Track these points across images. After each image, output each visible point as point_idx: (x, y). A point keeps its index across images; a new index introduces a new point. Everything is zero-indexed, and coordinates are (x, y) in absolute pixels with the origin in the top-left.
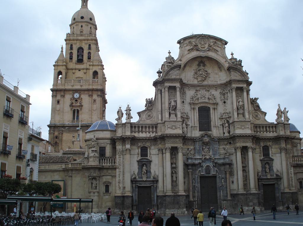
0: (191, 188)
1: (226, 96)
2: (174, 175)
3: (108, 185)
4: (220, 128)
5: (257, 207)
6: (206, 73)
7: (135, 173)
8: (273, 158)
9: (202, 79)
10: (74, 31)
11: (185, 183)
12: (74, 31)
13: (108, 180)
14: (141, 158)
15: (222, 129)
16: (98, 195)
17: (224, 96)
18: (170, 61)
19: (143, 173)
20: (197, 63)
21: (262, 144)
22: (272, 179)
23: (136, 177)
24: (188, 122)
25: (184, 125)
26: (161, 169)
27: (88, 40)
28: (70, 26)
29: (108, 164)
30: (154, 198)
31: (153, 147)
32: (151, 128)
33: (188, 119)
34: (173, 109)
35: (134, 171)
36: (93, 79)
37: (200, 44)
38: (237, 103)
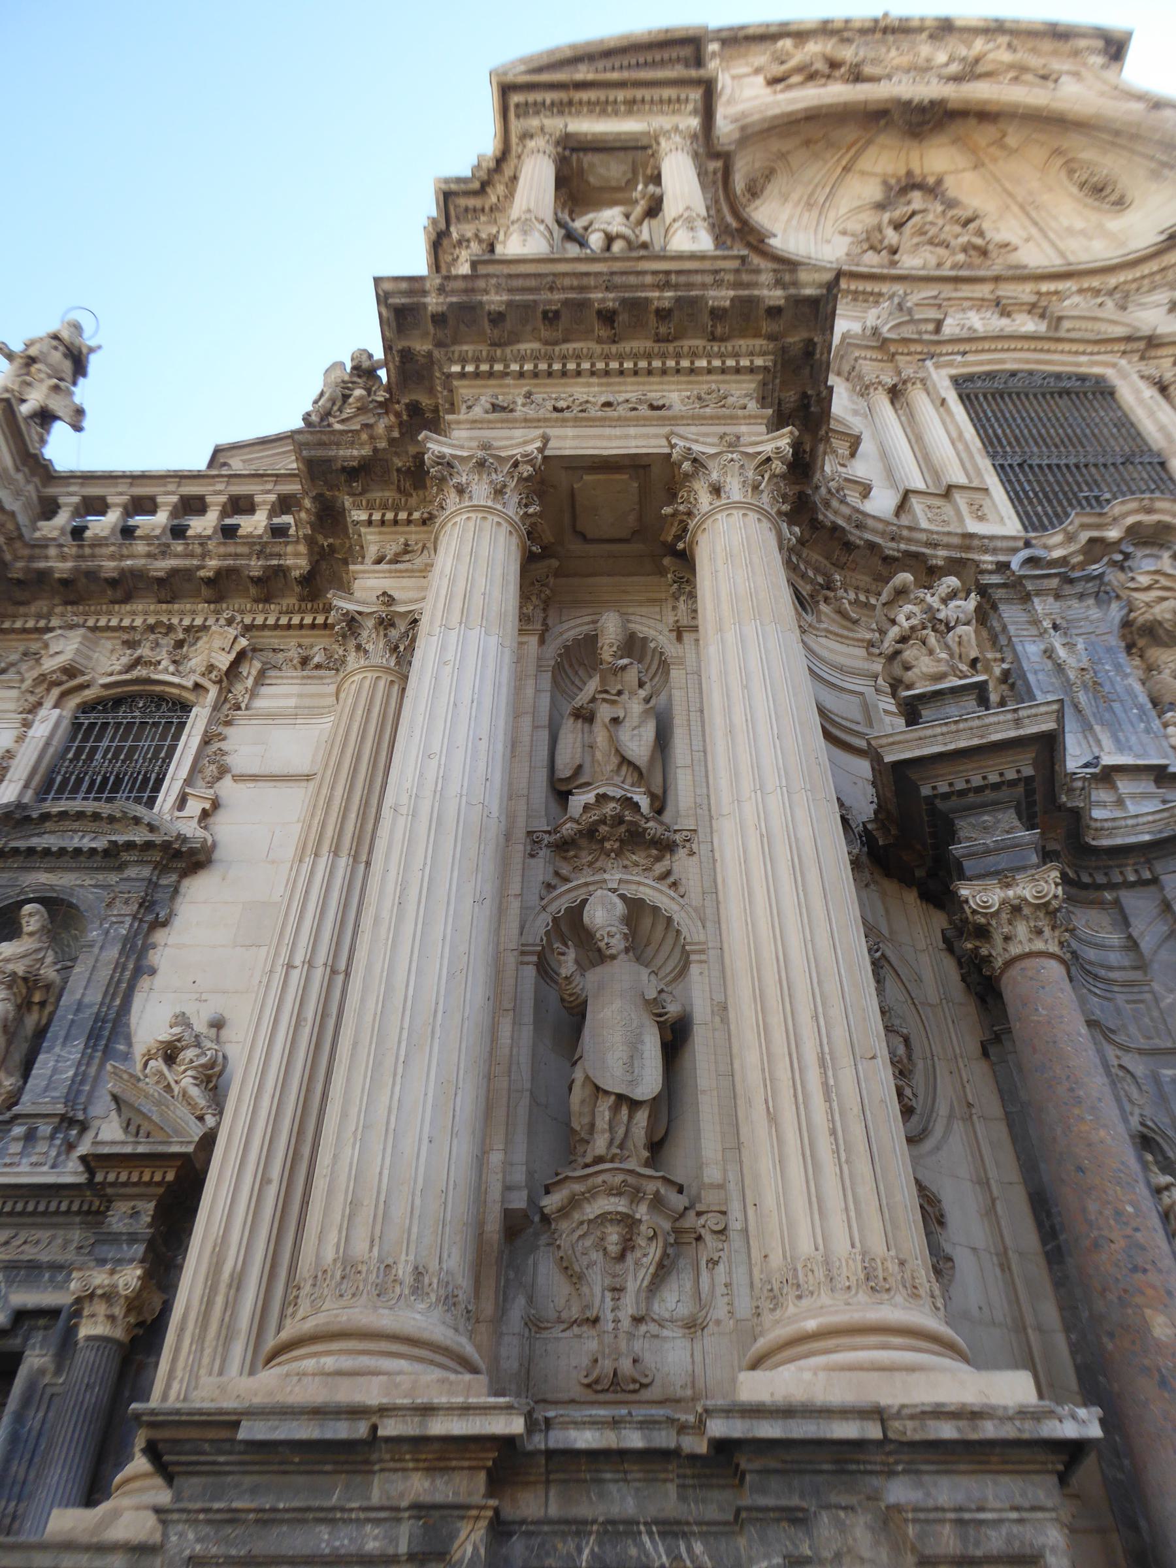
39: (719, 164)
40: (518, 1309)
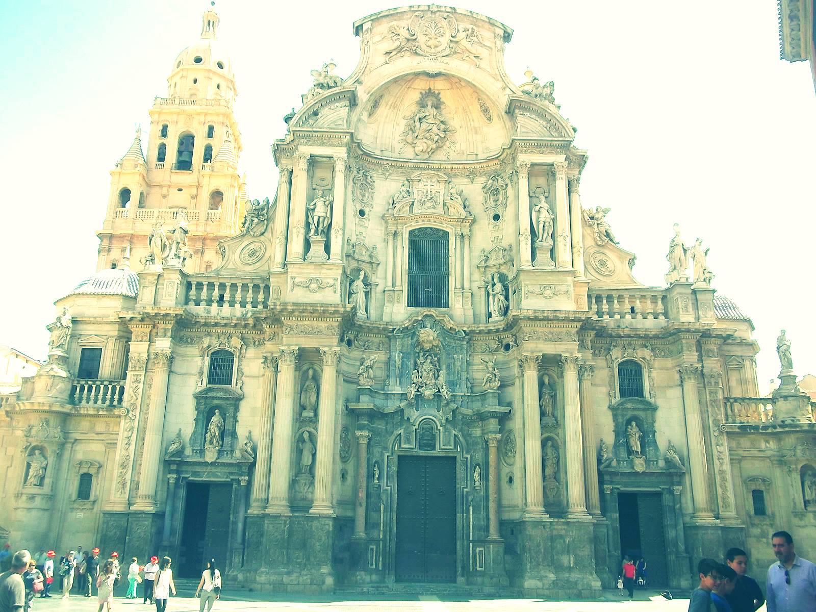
0: (360, 495)
1: (500, 197)
2: (307, 447)
3: (91, 476)
4: (477, 300)
5: (592, 574)
6: (442, 126)
7: (183, 436)
8: (660, 402)
9: (428, 147)
11: (344, 476)
13: (91, 457)
14: (209, 386)
15: (483, 302)
16: (46, 508)
17: (496, 198)
18: (322, 82)
19: (208, 435)
20: (414, 96)
21: (617, 355)
22: (652, 474)
23: (183, 448)
24: (374, 278)
25: (359, 285)
26: (267, 421)
29: (100, 402)
30: (235, 523)
31: (251, 352)
32: (250, 291)
33: (375, 266)
34: (320, 228)
35: (180, 430)
37: (426, 35)
38: (534, 214)
39: (356, 145)
40: (293, 490)
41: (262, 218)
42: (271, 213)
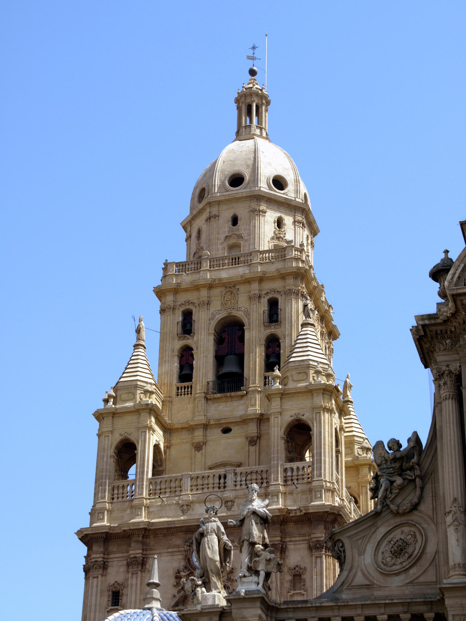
10: (200, 249)
12: (200, 249)
27: (261, 279)
28: (185, 228)
36: (288, 465)
41: (409, 475)
42: (426, 464)
